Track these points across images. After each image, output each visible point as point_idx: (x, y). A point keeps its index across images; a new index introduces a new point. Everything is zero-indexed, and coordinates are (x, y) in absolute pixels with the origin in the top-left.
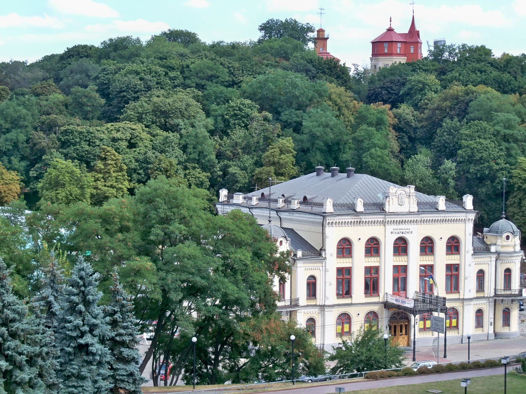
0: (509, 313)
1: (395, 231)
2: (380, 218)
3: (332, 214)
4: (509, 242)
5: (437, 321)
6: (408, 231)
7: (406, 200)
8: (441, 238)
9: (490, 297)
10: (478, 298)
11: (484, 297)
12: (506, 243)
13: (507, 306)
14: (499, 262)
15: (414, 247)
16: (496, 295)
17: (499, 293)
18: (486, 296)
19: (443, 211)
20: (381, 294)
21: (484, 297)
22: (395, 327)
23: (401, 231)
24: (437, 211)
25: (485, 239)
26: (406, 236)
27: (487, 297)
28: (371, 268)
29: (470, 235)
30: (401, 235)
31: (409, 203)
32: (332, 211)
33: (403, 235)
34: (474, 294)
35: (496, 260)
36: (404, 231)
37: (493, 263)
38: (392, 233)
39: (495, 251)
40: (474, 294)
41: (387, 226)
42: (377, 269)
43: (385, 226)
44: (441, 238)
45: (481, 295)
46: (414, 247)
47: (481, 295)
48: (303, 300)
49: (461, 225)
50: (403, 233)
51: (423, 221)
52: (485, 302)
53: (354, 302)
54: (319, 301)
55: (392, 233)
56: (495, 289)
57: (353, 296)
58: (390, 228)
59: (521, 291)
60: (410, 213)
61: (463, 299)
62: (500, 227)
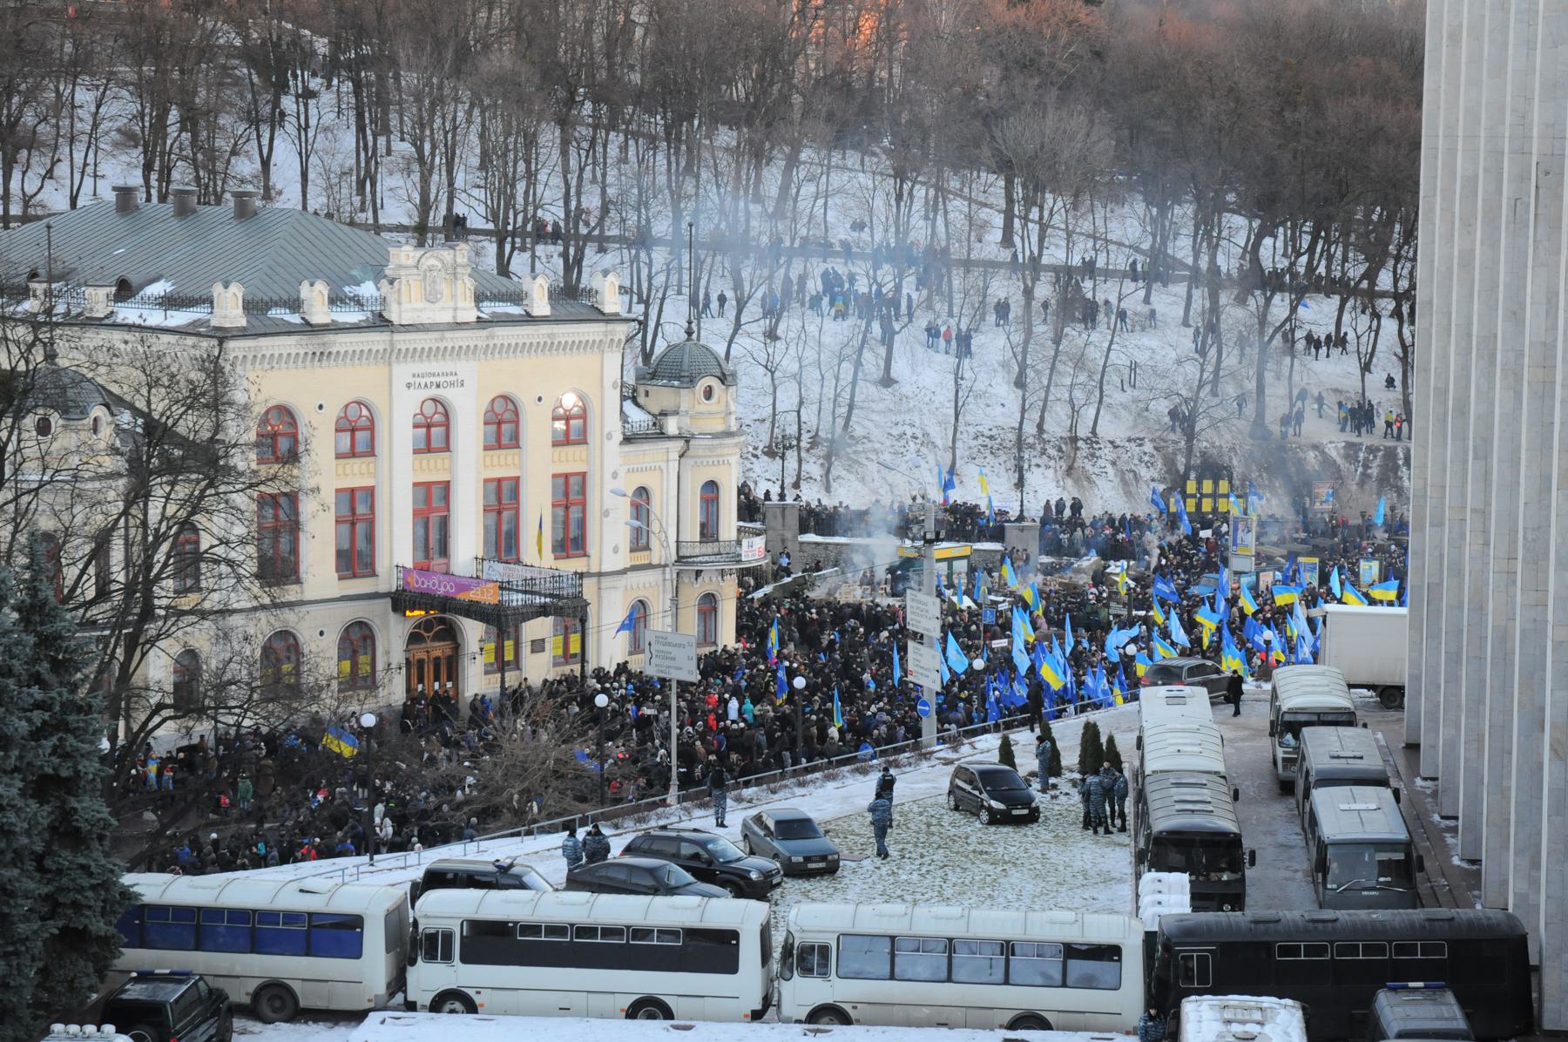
0: (715, 609)
1: (418, 380)
2: (378, 340)
3: (243, 334)
5: (669, 644)
7: (444, 287)
8: (540, 399)
9: (666, 566)
11: (650, 566)
12: (705, 406)
13: (710, 589)
15: (469, 430)
16: (680, 559)
17: (683, 552)
18: (655, 562)
19: (544, 320)
20: (382, 564)
21: (650, 566)
23: (434, 380)
24: (529, 319)
25: (641, 400)
26: (447, 394)
27: (659, 566)
28: (352, 491)
30: (433, 392)
31: (454, 297)
32: (243, 322)
35: (681, 456)
36: (441, 379)
37: (674, 466)
38: (409, 386)
40: (623, 559)
41: (395, 366)
42: (370, 492)
43: (390, 364)
45: (642, 558)
46: (469, 430)
47: (642, 558)
50: (438, 386)
51: (489, 351)
53: (308, 596)
55: (409, 386)
56: (678, 542)
57: (303, 575)
58: (404, 371)
59: (739, 543)
60: (459, 326)
61: (600, 575)
62: (686, 360)
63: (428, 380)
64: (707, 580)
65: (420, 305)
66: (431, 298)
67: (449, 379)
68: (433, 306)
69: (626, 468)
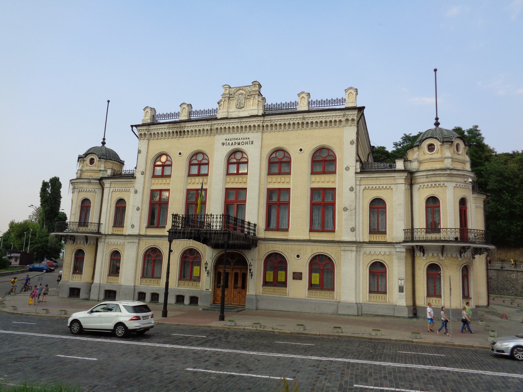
0: (440, 274)
1: (228, 142)
4: (435, 155)
6: (247, 141)
8: (301, 150)
10: (370, 243)
13: (434, 261)
14: (416, 187)
18: (388, 241)
21: (385, 243)
22: (227, 274)
23: (237, 141)
29: (352, 143)
30: (237, 146)
33: (240, 147)
34: (364, 235)
36: (241, 141)
38: (223, 144)
39: (403, 168)
40: (366, 237)
44: (301, 150)
48: (107, 227)
50: (239, 144)
54: (127, 230)
55: (223, 144)
58: (220, 138)
63: (233, 142)
64: (430, 255)
66: (238, 106)
67: (245, 141)
68: (239, 110)
69: (363, 187)
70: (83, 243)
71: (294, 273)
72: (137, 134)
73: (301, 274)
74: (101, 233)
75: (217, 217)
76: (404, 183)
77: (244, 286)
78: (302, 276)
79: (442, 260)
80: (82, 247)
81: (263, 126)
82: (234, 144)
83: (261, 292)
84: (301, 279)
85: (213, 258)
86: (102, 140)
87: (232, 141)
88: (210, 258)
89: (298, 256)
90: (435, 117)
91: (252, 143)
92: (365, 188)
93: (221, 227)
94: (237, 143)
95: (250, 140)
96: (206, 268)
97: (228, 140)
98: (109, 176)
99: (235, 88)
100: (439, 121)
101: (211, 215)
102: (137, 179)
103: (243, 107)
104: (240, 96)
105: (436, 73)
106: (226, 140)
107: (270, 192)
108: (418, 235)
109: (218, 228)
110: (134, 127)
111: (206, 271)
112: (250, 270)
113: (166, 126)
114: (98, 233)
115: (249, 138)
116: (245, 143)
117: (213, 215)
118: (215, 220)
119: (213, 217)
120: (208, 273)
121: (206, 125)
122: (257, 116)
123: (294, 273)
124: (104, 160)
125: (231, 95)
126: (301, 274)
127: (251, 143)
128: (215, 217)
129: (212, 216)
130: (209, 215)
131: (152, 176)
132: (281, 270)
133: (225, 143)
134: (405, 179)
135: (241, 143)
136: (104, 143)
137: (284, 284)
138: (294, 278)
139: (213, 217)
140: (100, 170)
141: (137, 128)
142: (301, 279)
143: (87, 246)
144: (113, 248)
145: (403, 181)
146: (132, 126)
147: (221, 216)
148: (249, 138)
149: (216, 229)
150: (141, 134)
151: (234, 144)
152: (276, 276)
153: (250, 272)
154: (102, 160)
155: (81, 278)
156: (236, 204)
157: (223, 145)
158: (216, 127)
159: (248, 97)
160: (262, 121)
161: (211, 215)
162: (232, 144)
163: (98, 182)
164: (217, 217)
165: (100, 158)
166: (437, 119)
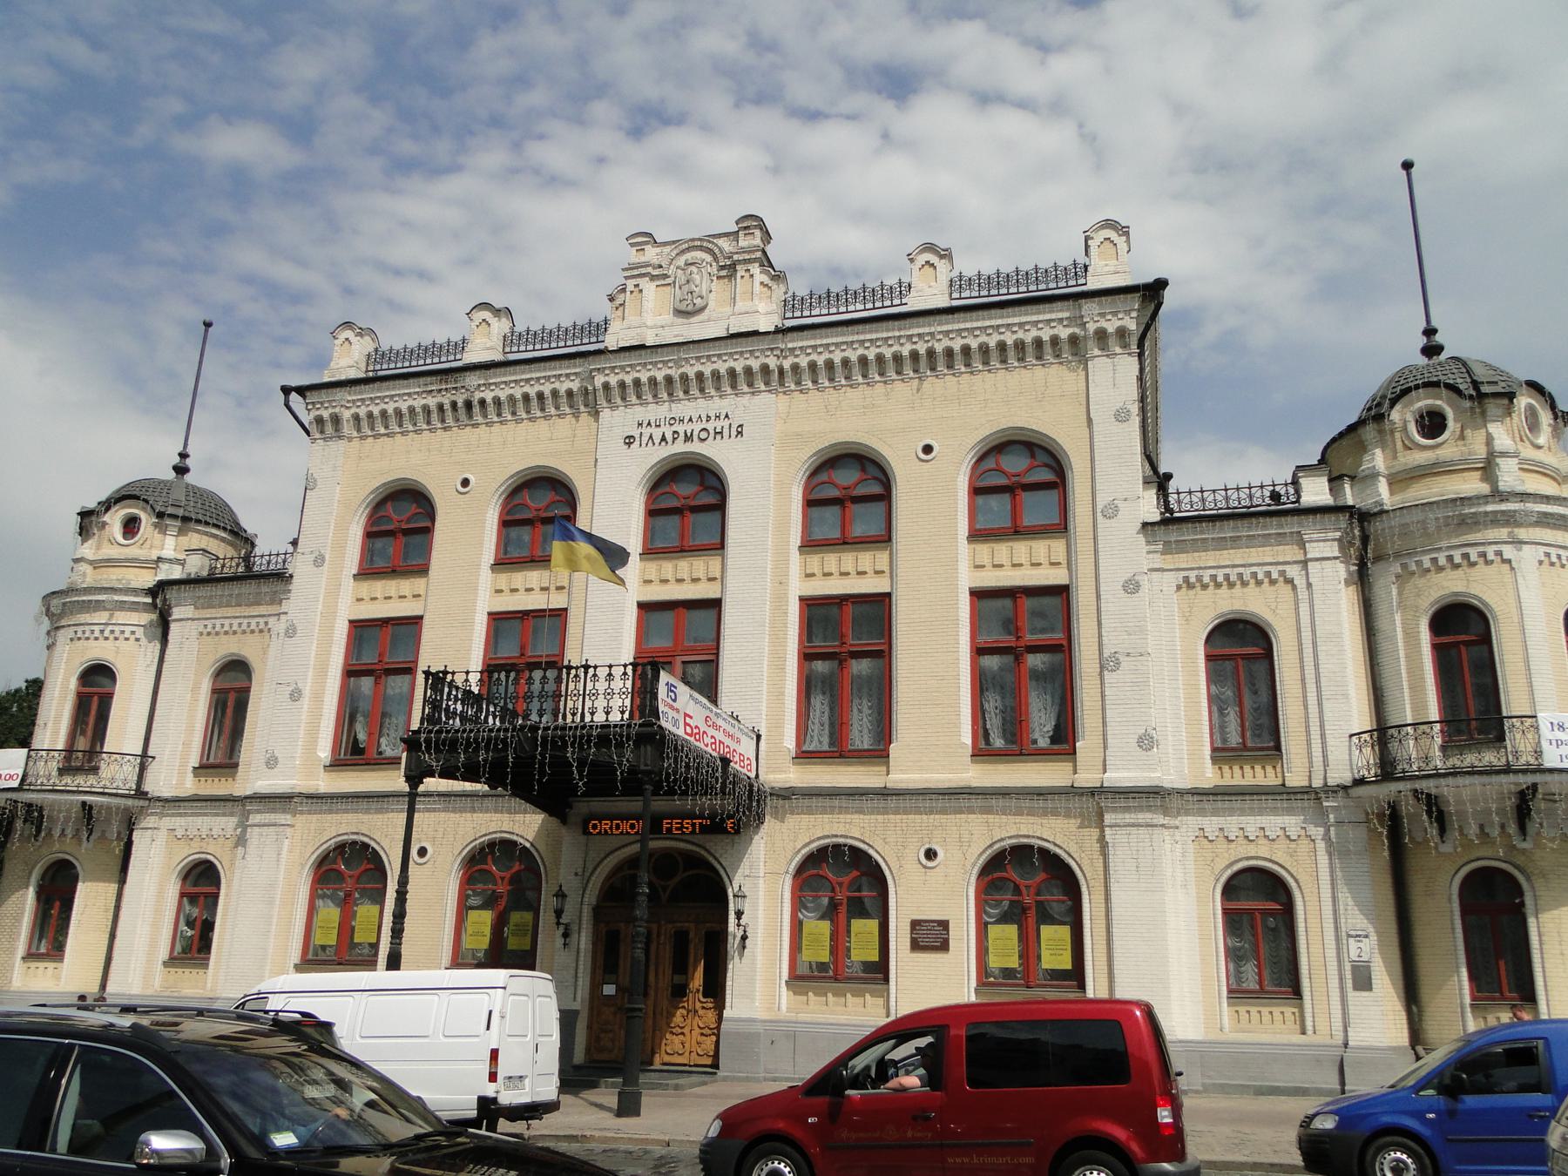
1: (647, 431)
6: (719, 425)
8: (928, 449)
18: (1296, 779)
27: (1307, 792)
29: (1121, 416)
30: (680, 447)
33: (695, 447)
38: (629, 441)
41: (605, 414)
49: (1056, 377)
50: (688, 438)
52: (1293, 823)
54: (253, 778)
55: (629, 441)
58: (618, 420)
65: (668, 317)
66: (683, 307)
70: (77, 833)
71: (915, 924)
72: (306, 419)
73: (944, 925)
74: (147, 793)
75: (610, 674)
76: (1337, 554)
77: (715, 989)
78: (948, 934)
79: (1524, 851)
80: (68, 850)
81: (781, 371)
82: (669, 437)
83: (784, 1007)
84: (944, 946)
85: (587, 874)
86: (177, 459)
87: (663, 429)
88: (576, 874)
89: (931, 854)
90: (1424, 324)
91: (740, 433)
92: (1186, 579)
93: (626, 716)
94: (682, 435)
95: (731, 421)
96: (559, 913)
97: (649, 424)
98: (192, 576)
99: (674, 242)
100: (1439, 338)
101: (586, 667)
102: (296, 585)
103: (702, 309)
104: (694, 269)
105: (1409, 176)
106: (640, 425)
107: (818, 612)
108: (1409, 751)
109: (615, 717)
110: (294, 396)
111: (558, 924)
112: (739, 914)
113: (414, 387)
114: (140, 793)
115: (727, 416)
116: (712, 434)
117: (595, 667)
118: (602, 686)
119: (595, 675)
120: (566, 935)
121: (567, 380)
122: (755, 333)
123: (915, 924)
124: (178, 523)
125: (661, 267)
126: (944, 925)
127: (734, 433)
128: (602, 672)
129: (591, 671)
130: (577, 668)
131: (355, 571)
132: (864, 914)
133: (637, 436)
134: (1339, 540)
135: (696, 433)
136: (181, 470)
137: (878, 971)
138: (916, 946)
139: (595, 675)
140: (160, 559)
141: (305, 399)
142: (944, 946)
143: (90, 845)
144: (186, 854)
145: (1333, 550)
146: (286, 390)
147: (629, 669)
148: (727, 416)
149: (607, 720)
150: (319, 421)
151: (669, 437)
152: (838, 944)
153: (739, 925)
154: (168, 522)
155: (58, 978)
156: (679, 659)
157: (629, 444)
158: (599, 380)
159: (724, 273)
160: (778, 352)
161: (586, 667)
162: (664, 439)
163: (149, 600)
164: (610, 674)
165: (160, 515)
166: (1430, 332)
